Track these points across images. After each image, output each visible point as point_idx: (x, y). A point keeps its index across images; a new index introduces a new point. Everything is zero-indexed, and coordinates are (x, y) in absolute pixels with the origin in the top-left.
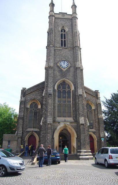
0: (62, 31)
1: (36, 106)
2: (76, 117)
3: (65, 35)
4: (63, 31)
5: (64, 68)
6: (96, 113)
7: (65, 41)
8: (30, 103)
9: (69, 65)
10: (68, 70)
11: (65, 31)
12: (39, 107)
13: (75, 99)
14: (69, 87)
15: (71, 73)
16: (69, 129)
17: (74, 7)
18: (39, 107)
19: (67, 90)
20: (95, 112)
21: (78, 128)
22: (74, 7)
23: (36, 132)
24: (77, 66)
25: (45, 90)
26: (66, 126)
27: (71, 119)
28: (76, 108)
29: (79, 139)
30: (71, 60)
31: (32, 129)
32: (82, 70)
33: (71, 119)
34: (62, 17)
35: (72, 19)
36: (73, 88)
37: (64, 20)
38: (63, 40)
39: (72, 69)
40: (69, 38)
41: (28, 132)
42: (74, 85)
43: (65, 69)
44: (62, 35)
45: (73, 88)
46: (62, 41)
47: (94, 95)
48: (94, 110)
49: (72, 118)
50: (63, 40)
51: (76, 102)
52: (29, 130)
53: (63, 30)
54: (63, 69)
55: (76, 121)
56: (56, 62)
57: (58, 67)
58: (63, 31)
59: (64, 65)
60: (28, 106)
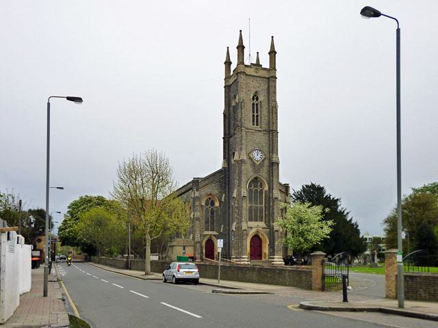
0: (253, 99)
1: (213, 204)
3: (257, 105)
4: (255, 97)
5: (257, 161)
7: (257, 116)
8: (206, 199)
9: (264, 157)
10: (262, 164)
12: (217, 204)
14: (261, 186)
15: (265, 169)
16: (260, 235)
17: (273, 53)
18: (217, 204)
21: (272, 234)
22: (273, 53)
23: (214, 235)
24: (274, 160)
26: (258, 231)
27: (262, 224)
29: (272, 246)
30: (266, 149)
31: (210, 233)
32: (278, 164)
33: (262, 224)
34: (255, 74)
35: (268, 78)
37: (259, 79)
38: (256, 114)
39: (266, 163)
41: (205, 235)
42: (269, 184)
44: (253, 104)
45: (266, 188)
46: (253, 115)
49: (263, 223)
50: (256, 114)
52: (206, 233)
53: (256, 97)
55: (270, 227)
56: (248, 152)
57: (250, 158)
58: (255, 97)
59: (257, 156)
60: (203, 204)
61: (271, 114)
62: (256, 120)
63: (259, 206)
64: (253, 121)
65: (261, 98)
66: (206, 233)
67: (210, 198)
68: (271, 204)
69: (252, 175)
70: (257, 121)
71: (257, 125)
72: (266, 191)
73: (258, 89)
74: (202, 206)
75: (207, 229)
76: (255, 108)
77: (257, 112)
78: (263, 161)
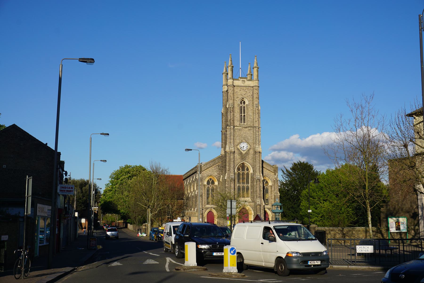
0: (241, 103)
1: (213, 182)
2: (253, 198)
3: (244, 107)
4: (243, 102)
5: (244, 151)
6: (273, 189)
7: (244, 116)
10: (247, 153)
11: (244, 103)
12: (216, 183)
13: (253, 182)
14: (248, 169)
15: (251, 156)
19: (246, 172)
20: (271, 189)
25: (227, 174)
28: (253, 190)
30: (251, 141)
34: (242, 85)
36: (251, 171)
37: (245, 88)
38: (243, 115)
39: (251, 152)
40: (249, 113)
41: (207, 208)
42: (253, 168)
43: (245, 152)
47: (272, 171)
48: (271, 186)
50: (243, 115)
51: (254, 185)
54: (242, 152)
55: (253, 201)
56: (236, 144)
57: (238, 149)
58: (243, 102)
59: (244, 146)
60: (205, 183)
61: (254, 114)
62: (243, 119)
63: (245, 185)
64: (241, 120)
65: (247, 103)
66: (208, 206)
67: (211, 179)
68: (255, 184)
69: (238, 161)
70: (244, 120)
71: (244, 122)
72: (251, 174)
73: (244, 96)
74: (204, 185)
75: (208, 203)
76: (242, 110)
77: (244, 113)
78: (249, 150)
